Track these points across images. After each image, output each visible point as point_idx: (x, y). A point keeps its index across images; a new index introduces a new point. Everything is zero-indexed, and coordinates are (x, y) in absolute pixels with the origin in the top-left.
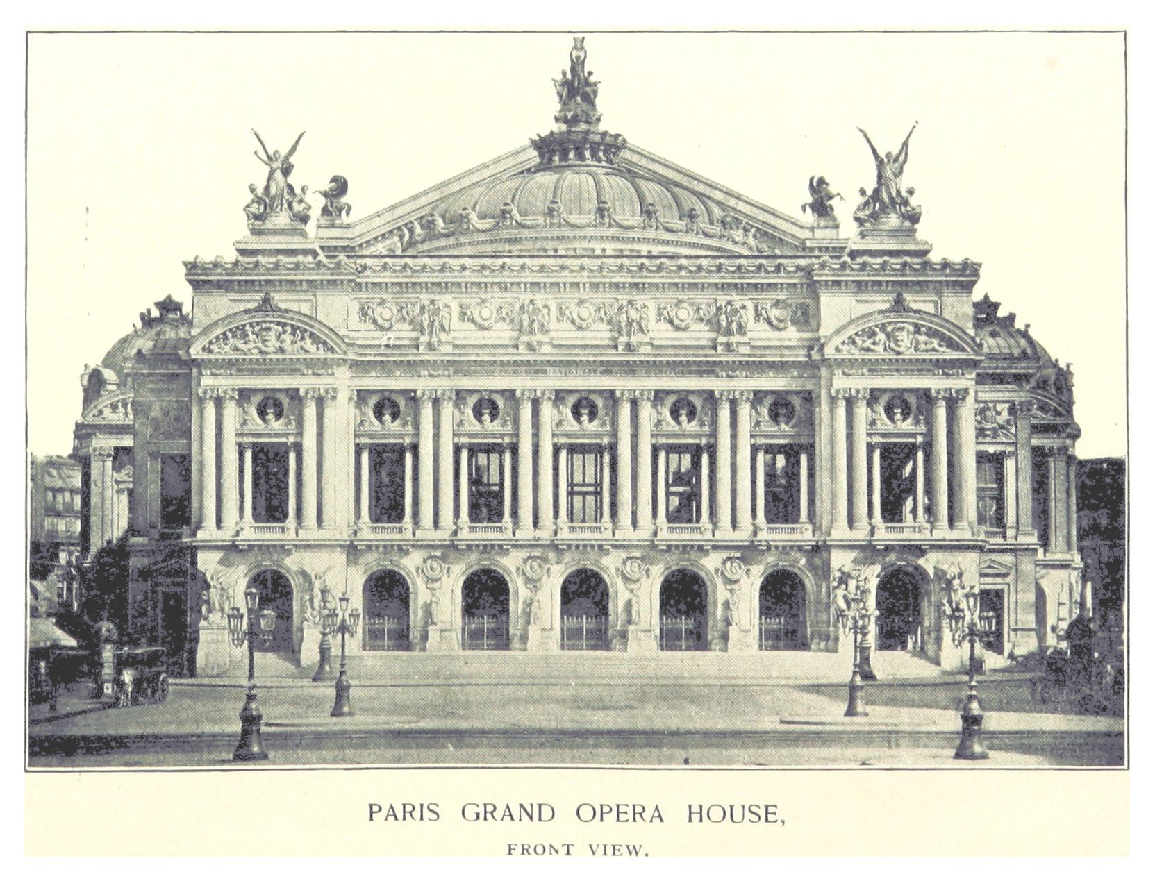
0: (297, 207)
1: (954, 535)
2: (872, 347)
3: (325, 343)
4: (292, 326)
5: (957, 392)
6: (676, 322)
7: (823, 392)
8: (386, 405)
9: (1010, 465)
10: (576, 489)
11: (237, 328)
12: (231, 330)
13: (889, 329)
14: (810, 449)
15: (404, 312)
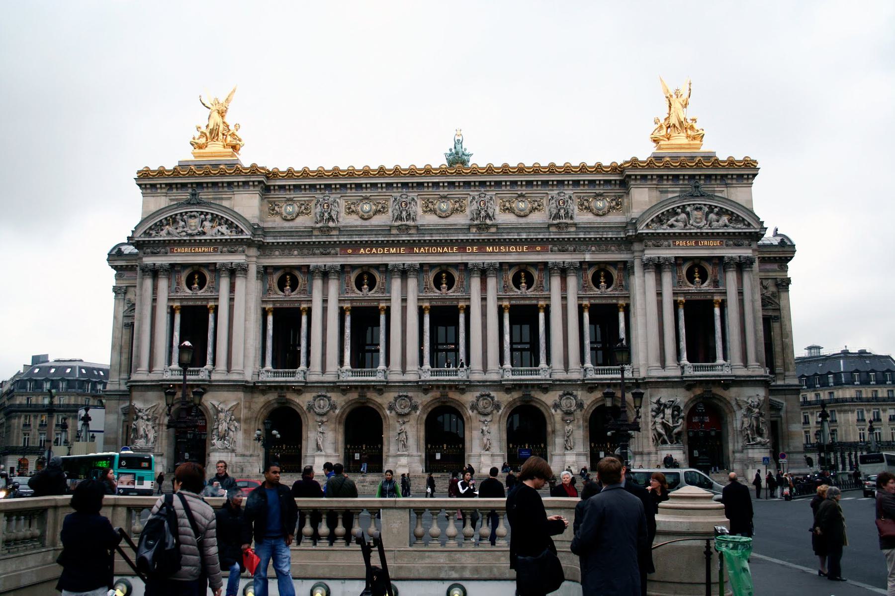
0: (229, 139)
1: (750, 373)
2: (675, 223)
3: (237, 227)
4: (212, 214)
5: (748, 258)
6: (516, 211)
7: (637, 263)
8: (288, 278)
9: (776, 326)
10: (440, 347)
11: (171, 216)
12: (166, 218)
13: (688, 209)
14: (627, 310)
15: (303, 207)
